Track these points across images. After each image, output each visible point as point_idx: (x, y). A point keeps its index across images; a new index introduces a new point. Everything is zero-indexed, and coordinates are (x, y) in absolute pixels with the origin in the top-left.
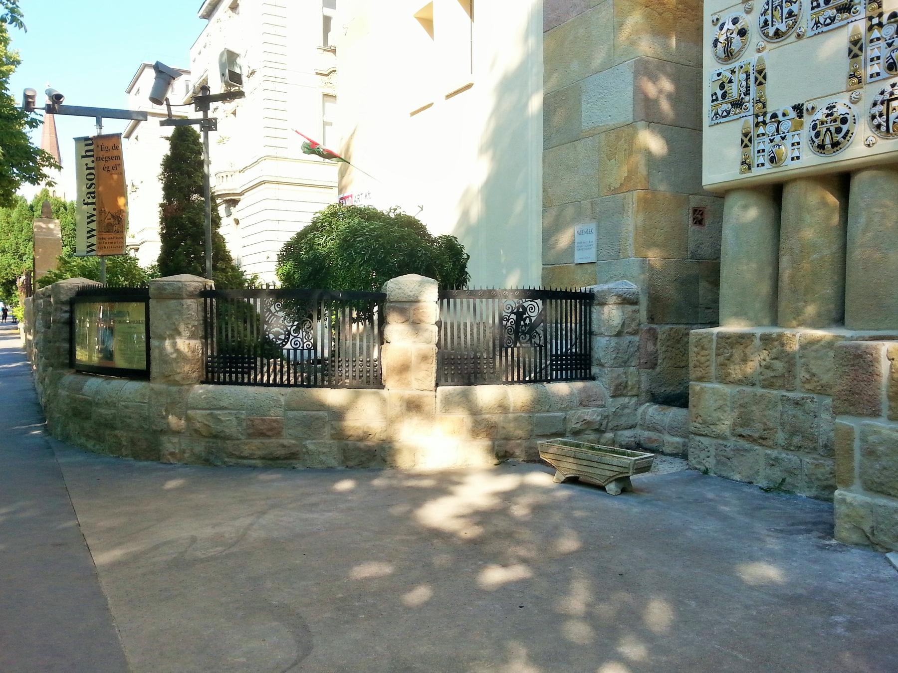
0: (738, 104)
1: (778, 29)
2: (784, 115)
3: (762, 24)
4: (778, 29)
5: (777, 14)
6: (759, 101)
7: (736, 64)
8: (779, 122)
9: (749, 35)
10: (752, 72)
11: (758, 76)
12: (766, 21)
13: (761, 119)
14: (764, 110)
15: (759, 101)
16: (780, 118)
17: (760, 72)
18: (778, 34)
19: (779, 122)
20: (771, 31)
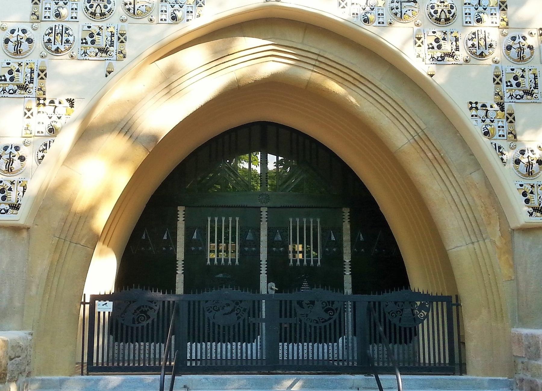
0: (23, 88)
1: (58, 48)
2: (60, 103)
3: (46, 41)
4: (58, 48)
5: (59, 38)
6: (40, 89)
7: (24, 61)
8: (56, 107)
9: (34, 44)
10: (35, 69)
11: (40, 73)
12: (49, 40)
13: (42, 102)
14: (44, 96)
15: (40, 89)
16: (57, 103)
17: (42, 71)
18: (57, 50)
19: (56, 107)
20: (54, 48)
